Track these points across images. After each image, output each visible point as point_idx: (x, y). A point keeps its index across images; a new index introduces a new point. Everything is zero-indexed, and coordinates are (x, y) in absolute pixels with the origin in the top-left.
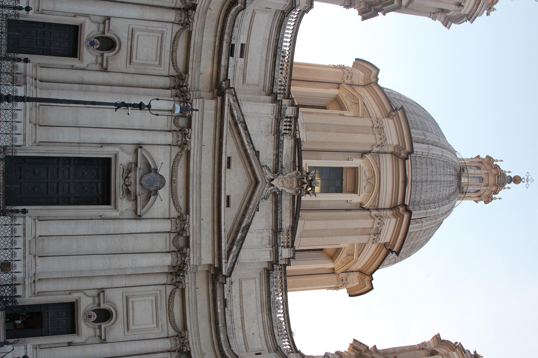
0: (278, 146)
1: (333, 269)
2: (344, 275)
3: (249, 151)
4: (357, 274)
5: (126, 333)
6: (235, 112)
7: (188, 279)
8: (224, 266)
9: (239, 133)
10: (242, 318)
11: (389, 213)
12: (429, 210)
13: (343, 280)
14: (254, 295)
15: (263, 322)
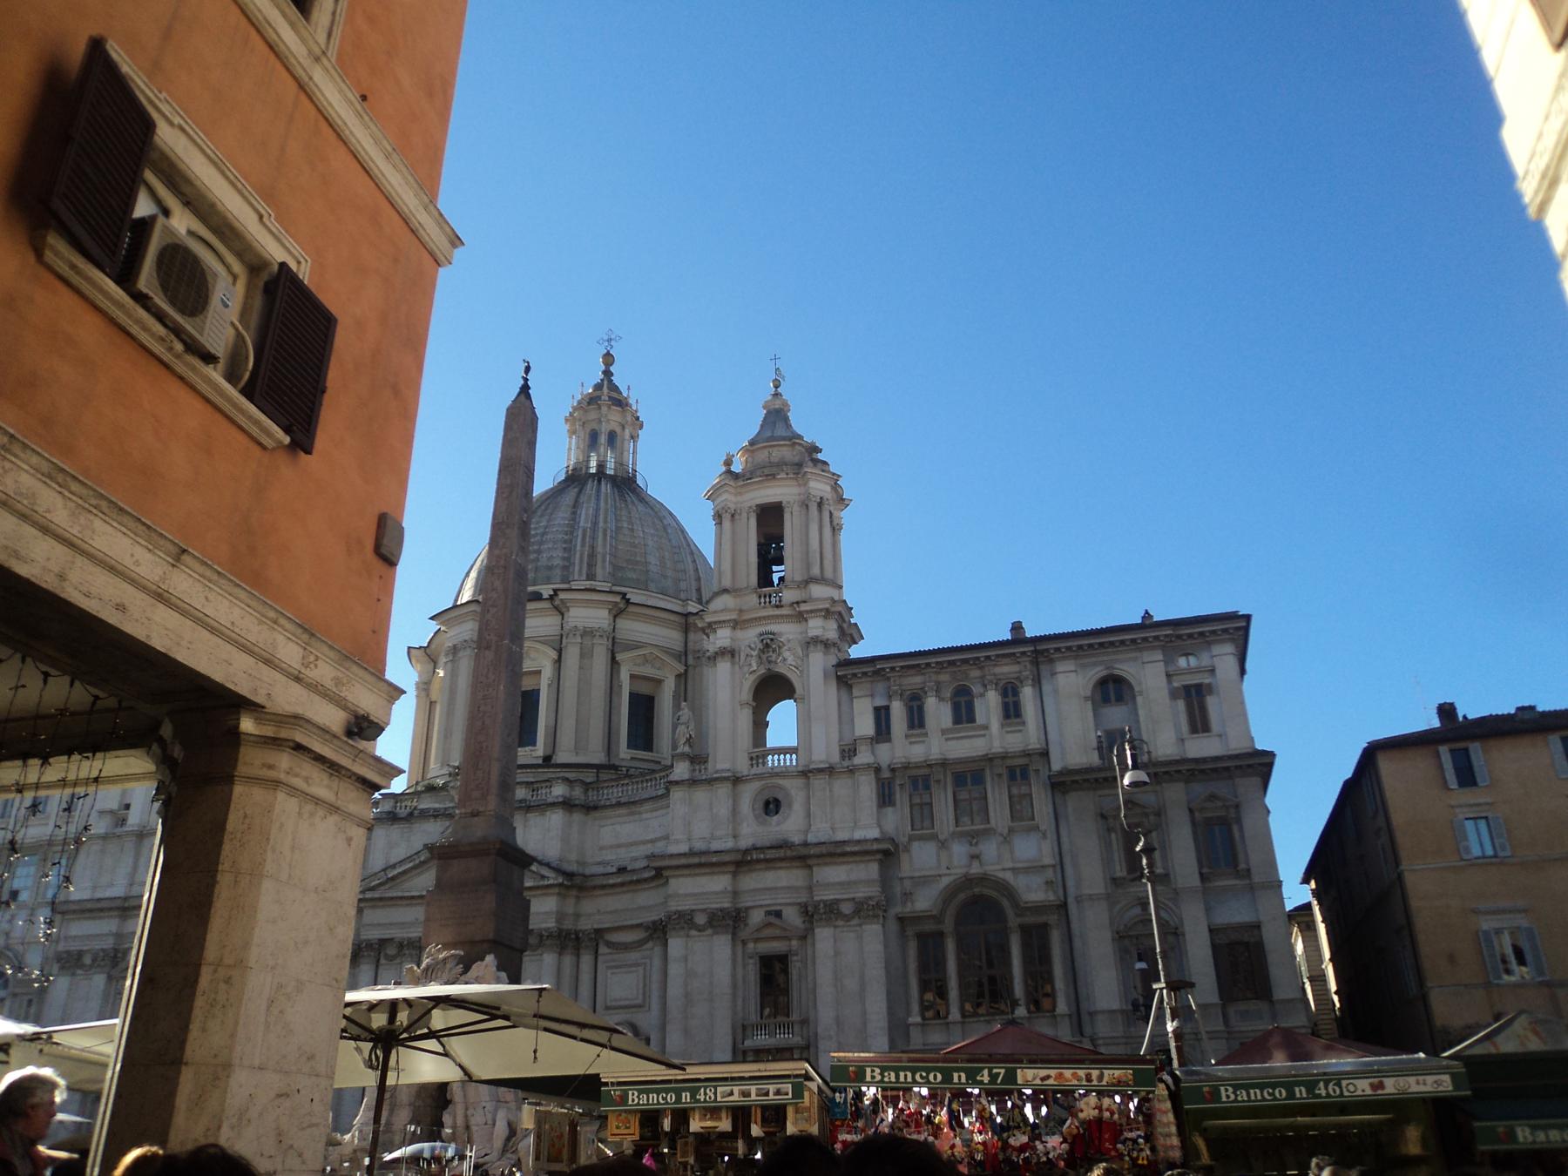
0: (425, 815)
1: (678, 676)
2: (690, 658)
3: (422, 859)
4: (692, 636)
5: (647, 1008)
6: (373, 884)
7: (586, 925)
8: (551, 882)
9: (404, 872)
10: (644, 842)
11: (566, 616)
12: (578, 548)
13: (699, 658)
14: (618, 827)
15: (652, 811)
